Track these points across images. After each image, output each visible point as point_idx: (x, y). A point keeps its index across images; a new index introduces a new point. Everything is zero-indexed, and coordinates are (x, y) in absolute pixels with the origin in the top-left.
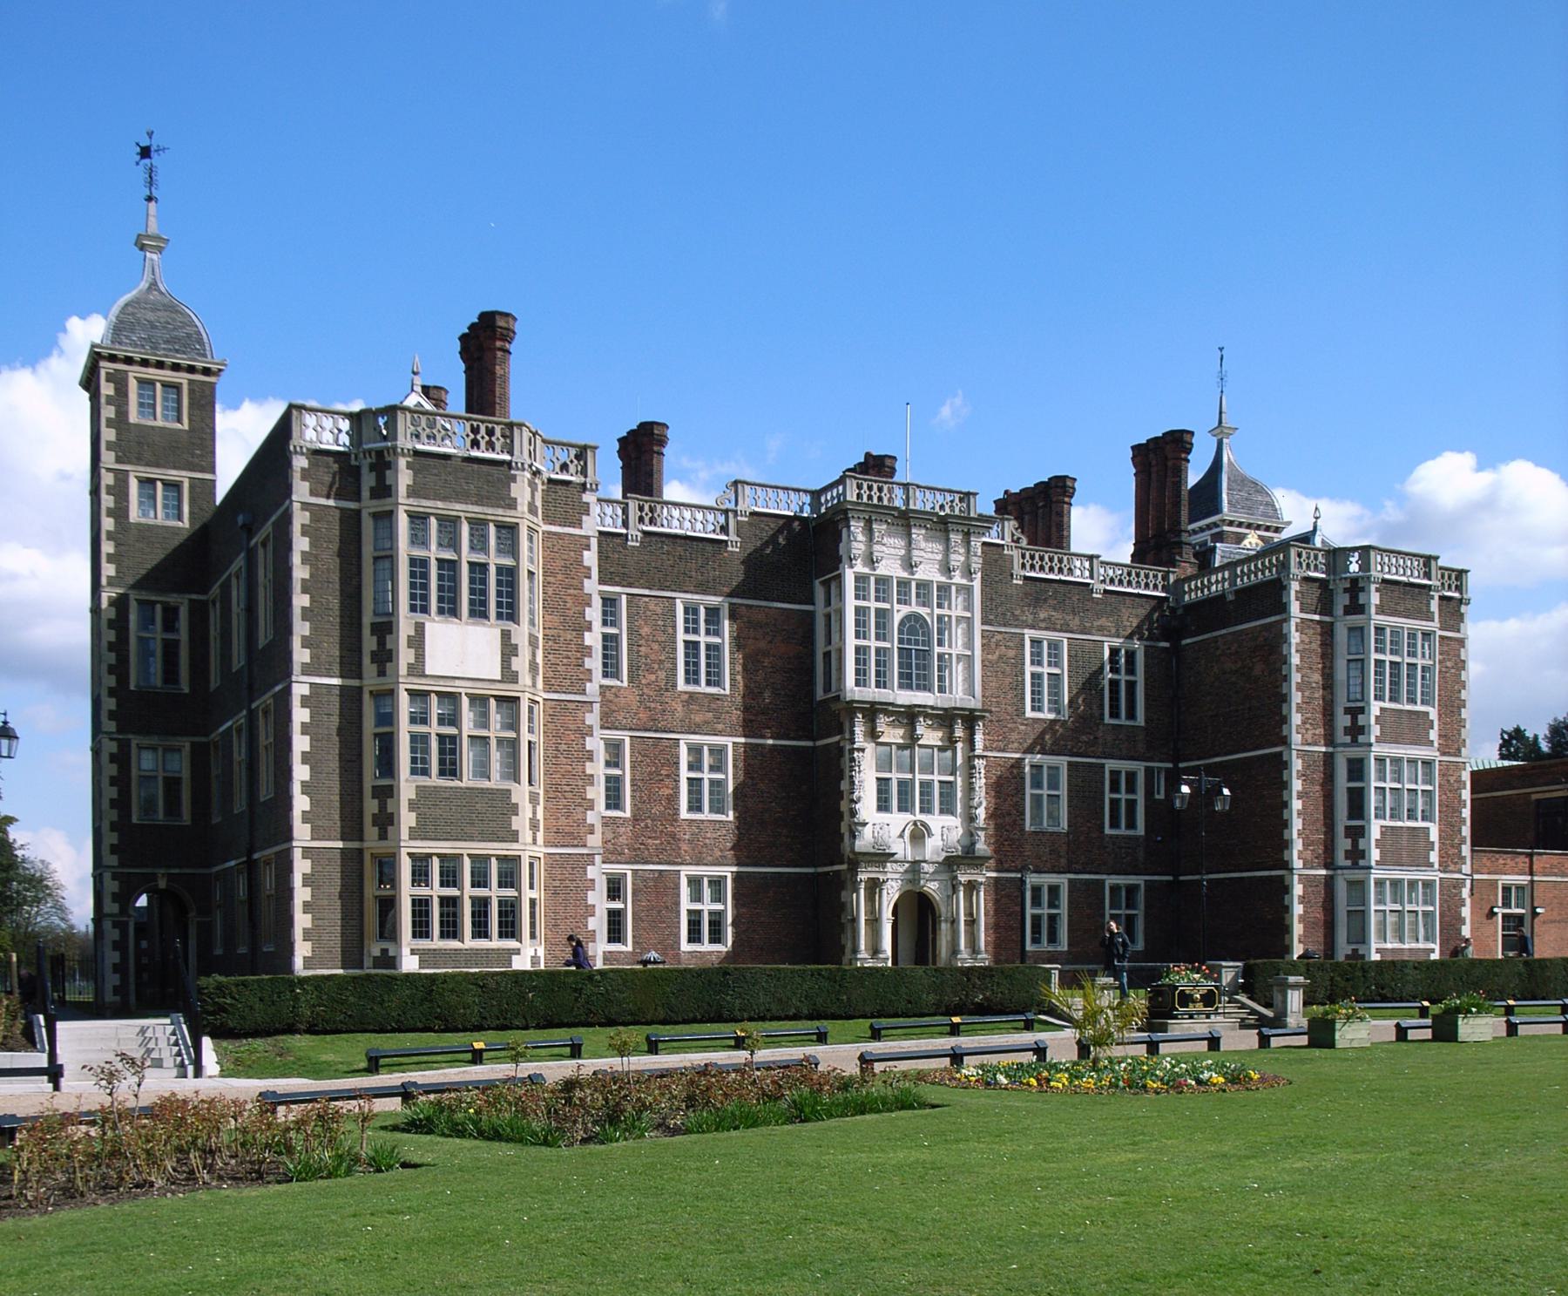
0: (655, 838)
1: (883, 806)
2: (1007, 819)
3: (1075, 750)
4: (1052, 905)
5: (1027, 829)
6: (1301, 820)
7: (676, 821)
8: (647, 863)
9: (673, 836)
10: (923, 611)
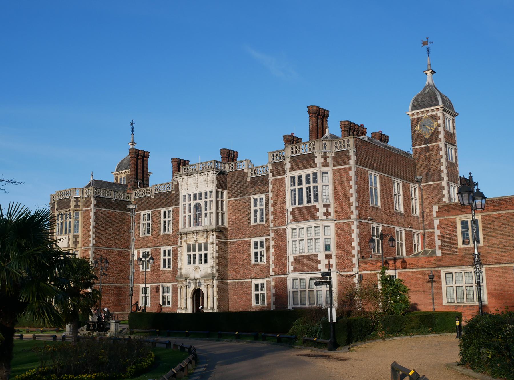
0: (155, 276)
1: (189, 263)
2: (246, 261)
3: (268, 234)
4: (262, 290)
5: (252, 264)
6: (273, 257)
7: (160, 271)
8: (153, 283)
9: (159, 275)
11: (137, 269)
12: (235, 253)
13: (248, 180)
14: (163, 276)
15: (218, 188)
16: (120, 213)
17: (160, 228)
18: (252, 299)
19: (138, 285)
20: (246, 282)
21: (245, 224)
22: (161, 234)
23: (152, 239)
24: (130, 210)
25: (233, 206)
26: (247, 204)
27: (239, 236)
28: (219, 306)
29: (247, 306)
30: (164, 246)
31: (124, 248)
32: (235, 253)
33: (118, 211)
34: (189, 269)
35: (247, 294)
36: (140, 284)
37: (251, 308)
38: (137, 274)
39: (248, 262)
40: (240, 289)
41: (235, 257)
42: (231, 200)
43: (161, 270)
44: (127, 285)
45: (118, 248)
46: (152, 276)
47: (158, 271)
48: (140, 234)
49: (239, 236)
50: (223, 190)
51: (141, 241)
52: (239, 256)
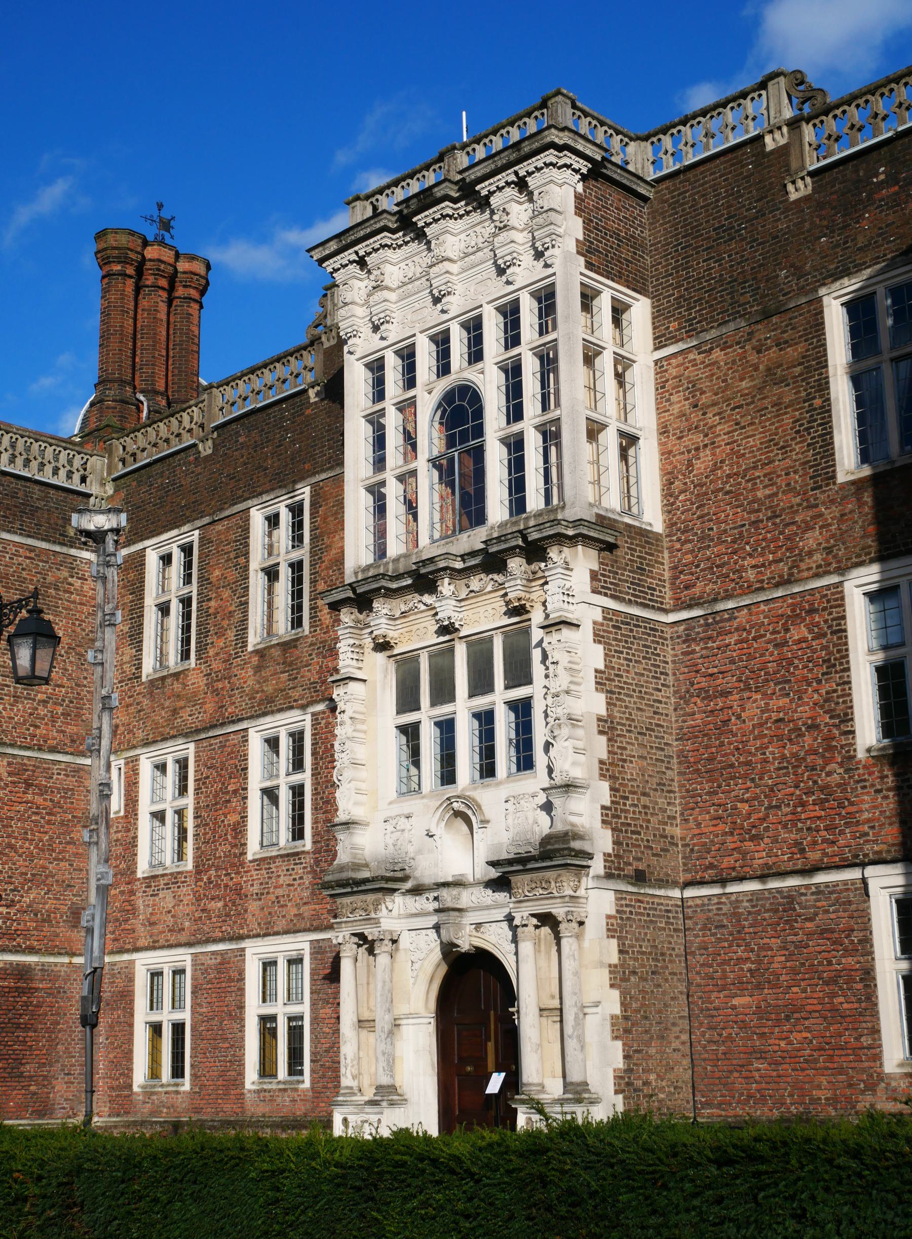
2: (808, 740)
5: (861, 755)
7: (242, 864)
8: (208, 941)
9: (238, 891)
10: (472, 375)
11: (123, 866)
12: (725, 694)
13: (793, 196)
14: (259, 896)
15: (589, 266)
16: (31, 549)
17: (245, 612)
18: (875, 1015)
19: (126, 957)
20: (819, 890)
21: (790, 489)
22: (250, 648)
23: (202, 682)
24: (96, 538)
25: (694, 389)
26: (792, 353)
27: (751, 575)
28: (629, 1071)
29: (841, 1071)
30: (265, 714)
31: (53, 750)
32: (725, 694)
33: (17, 538)
34: (403, 823)
35: (833, 981)
36: (137, 950)
37: (871, 1087)
38: (122, 892)
39: (830, 748)
40: (775, 943)
41: (726, 722)
42: (674, 355)
43: (250, 857)
44: (66, 960)
45: (12, 745)
46: (199, 900)
47: (233, 865)
48: (139, 667)
49: (751, 575)
50: (625, 293)
51: (146, 702)
52: (752, 711)
